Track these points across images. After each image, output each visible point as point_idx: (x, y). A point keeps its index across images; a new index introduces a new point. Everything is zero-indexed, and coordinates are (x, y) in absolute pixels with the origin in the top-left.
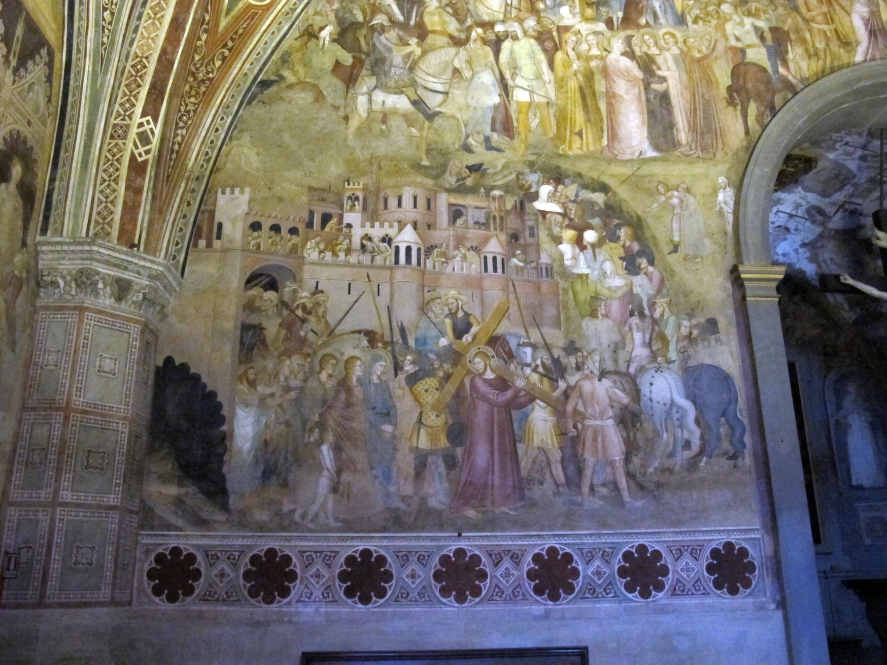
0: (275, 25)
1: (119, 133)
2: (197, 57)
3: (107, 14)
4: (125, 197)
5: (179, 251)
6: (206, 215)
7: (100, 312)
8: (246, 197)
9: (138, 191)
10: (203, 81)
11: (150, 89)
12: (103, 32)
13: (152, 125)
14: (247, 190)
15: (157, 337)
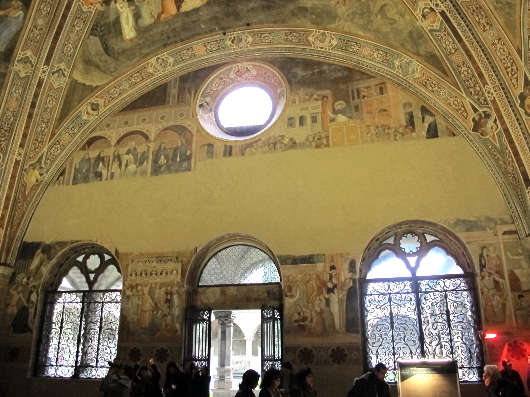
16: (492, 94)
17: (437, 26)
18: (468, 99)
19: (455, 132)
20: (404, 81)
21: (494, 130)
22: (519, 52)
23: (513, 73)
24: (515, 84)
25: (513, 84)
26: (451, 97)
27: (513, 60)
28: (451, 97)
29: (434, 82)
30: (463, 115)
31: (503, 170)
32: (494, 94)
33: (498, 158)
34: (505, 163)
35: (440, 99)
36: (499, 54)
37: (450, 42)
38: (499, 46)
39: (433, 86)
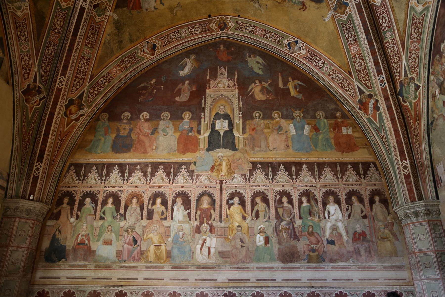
0: (423, 103)
1: (400, 171)
2: (413, 129)
3: (384, 140)
4: (407, 187)
5: (433, 192)
6: (437, 176)
7: (413, 223)
8: (442, 165)
9: (411, 183)
10: (417, 135)
11: (399, 153)
12: (385, 145)
13: (406, 162)
14: (441, 162)
15: (441, 221)
16: (62, 85)
17: (63, 6)
18: (36, 69)
19: (10, 82)
20: (4, 4)
21: (35, 104)
22: (92, 78)
23: (78, 84)
24: (73, 90)
25: (72, 89)
26: (27, 55)
27: (85, 77)
28: (27, 55)
29: (26, 33)
30: (24, 75)
31: (22, 137)
32: (64, 86)
33: (25, 125)
34: (26, 132)
35: (18, 48)
36: (80, 65)
37: (60, 24)
38: (85, 62)
39: (22, 34)
